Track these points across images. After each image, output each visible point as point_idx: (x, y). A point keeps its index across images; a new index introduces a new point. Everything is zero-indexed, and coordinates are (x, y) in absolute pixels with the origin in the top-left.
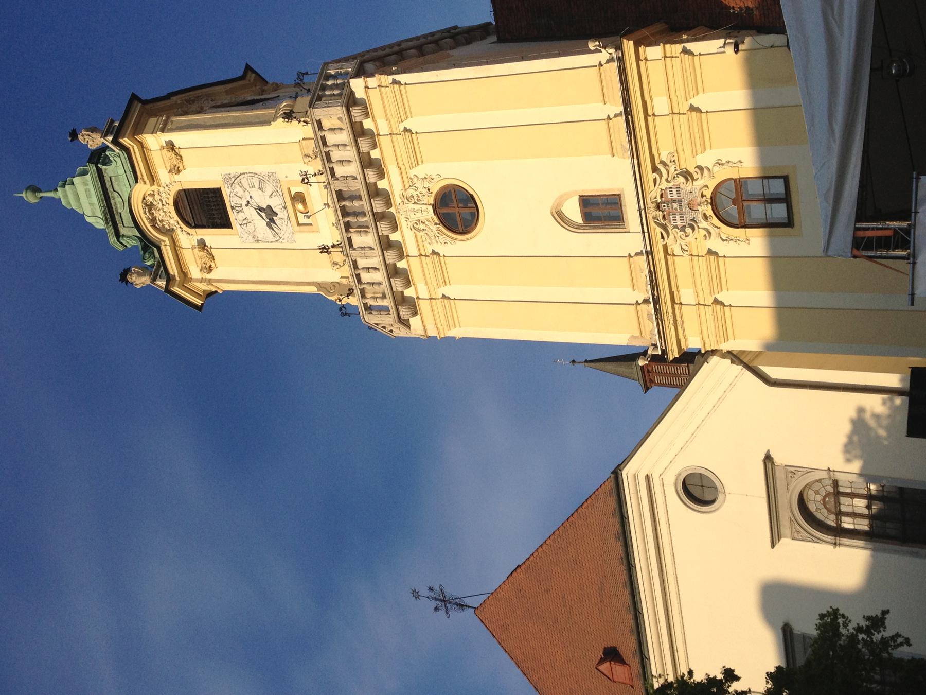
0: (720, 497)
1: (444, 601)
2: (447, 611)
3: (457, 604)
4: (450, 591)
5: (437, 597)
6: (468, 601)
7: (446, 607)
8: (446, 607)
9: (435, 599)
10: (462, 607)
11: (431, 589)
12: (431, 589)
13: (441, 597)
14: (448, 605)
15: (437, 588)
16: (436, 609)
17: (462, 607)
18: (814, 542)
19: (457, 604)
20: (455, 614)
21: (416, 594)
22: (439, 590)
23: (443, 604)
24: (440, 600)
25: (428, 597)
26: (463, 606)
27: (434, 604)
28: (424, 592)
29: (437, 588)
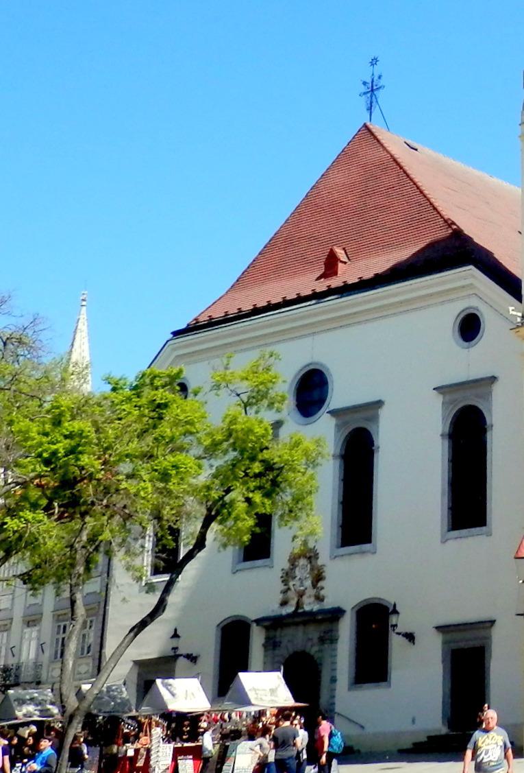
0: (466, 344)
1: (372, 90)
2: (365, 93)
3: (371, 103)
4: (380, 94)
5: (374, 83)
6: (376, 111)
8: (368, 92)
9: (373, 81)
10: (370, 109)
11: (380, 77)
12: (380, 77)
13: (375, 88)
14: (369, 95)
15: (382, 83)
16: (365, 83)
17: (370, 109)
18: (443, 419)
19: (371, 103)
20: (363, 102)
21: (374, 62)
22: (380, 85)
23: (370, 90)
24: (372, 86)
25: (373, 75)
26: (371, 109)
27: (369, 81)
28: (378, 69)
29: (382, 83)
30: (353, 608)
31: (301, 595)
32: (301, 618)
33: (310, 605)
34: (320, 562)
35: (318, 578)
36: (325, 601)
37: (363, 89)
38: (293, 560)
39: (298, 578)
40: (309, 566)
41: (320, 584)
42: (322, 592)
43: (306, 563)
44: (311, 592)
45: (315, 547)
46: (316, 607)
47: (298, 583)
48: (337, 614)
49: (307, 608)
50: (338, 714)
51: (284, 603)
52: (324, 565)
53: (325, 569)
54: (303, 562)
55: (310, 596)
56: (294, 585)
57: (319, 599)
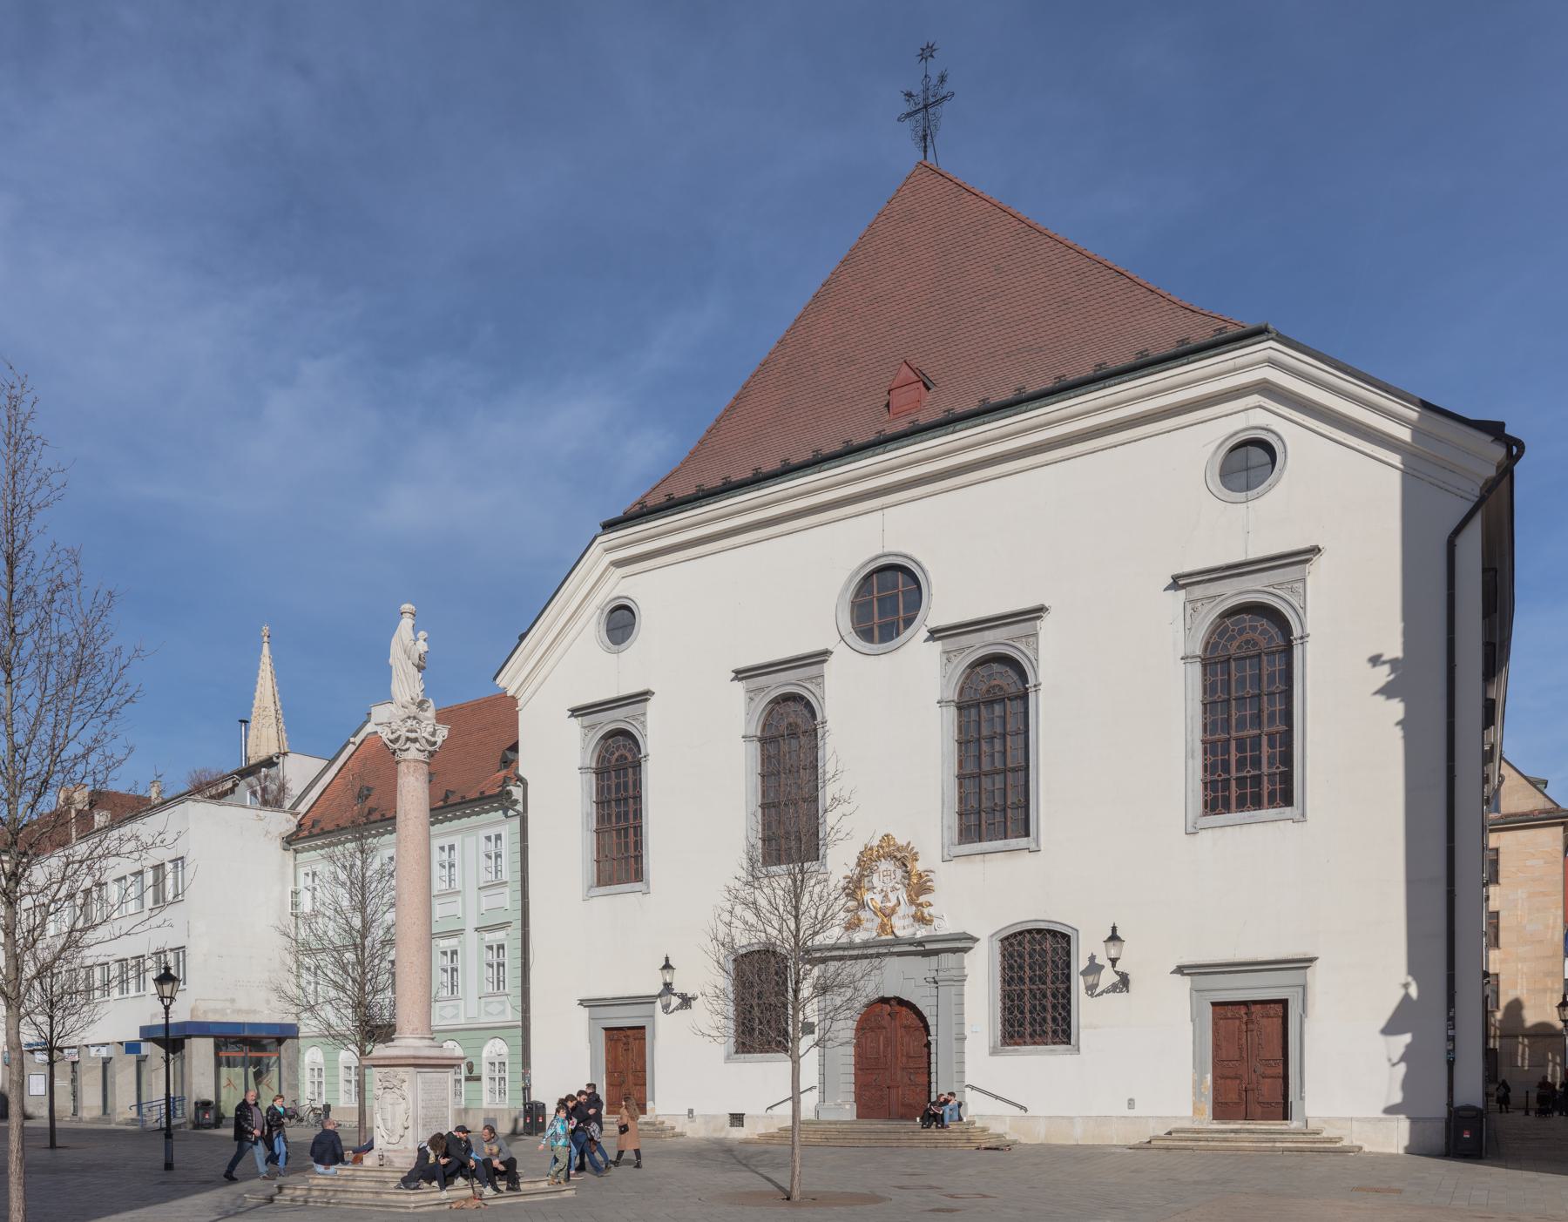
1: (926, 107)
2: (909, 115)
7: (916, 112)
8: (916, 112)
10: (925, 138)
14: (919, 116)
16: (909, 95)
17: (925, 138)
27: (917, 89)
30: (992, 936)
31: (888, 914)
32: (886, 948)
33: (903, 927)
34: (920, 866)
35: (919, 887)
36: (936, 922)
37: (907, 108)
38: (866, 862)
39: (879, 889)
40: (899, 873)
41: (922, 899)
42: (931, 910)
43: (892, 868)
44: (905, 909)
45: (909, 843)
46: (921, 932)
47: (878, 898)
48: (961, 944)
49: (899, 933)
50: (973, 1088)
51: (852, 926)
52: (932, 871)
53: (932, 876)
54: (885, 865)
55: (904, 917)
56: (872, 899)
57: (922, 920)
